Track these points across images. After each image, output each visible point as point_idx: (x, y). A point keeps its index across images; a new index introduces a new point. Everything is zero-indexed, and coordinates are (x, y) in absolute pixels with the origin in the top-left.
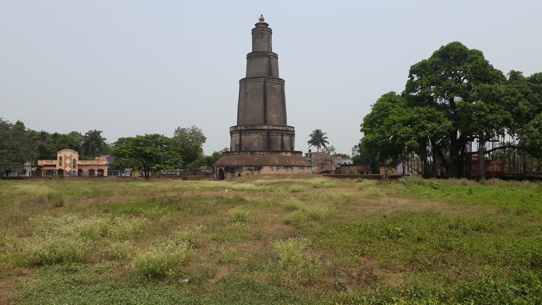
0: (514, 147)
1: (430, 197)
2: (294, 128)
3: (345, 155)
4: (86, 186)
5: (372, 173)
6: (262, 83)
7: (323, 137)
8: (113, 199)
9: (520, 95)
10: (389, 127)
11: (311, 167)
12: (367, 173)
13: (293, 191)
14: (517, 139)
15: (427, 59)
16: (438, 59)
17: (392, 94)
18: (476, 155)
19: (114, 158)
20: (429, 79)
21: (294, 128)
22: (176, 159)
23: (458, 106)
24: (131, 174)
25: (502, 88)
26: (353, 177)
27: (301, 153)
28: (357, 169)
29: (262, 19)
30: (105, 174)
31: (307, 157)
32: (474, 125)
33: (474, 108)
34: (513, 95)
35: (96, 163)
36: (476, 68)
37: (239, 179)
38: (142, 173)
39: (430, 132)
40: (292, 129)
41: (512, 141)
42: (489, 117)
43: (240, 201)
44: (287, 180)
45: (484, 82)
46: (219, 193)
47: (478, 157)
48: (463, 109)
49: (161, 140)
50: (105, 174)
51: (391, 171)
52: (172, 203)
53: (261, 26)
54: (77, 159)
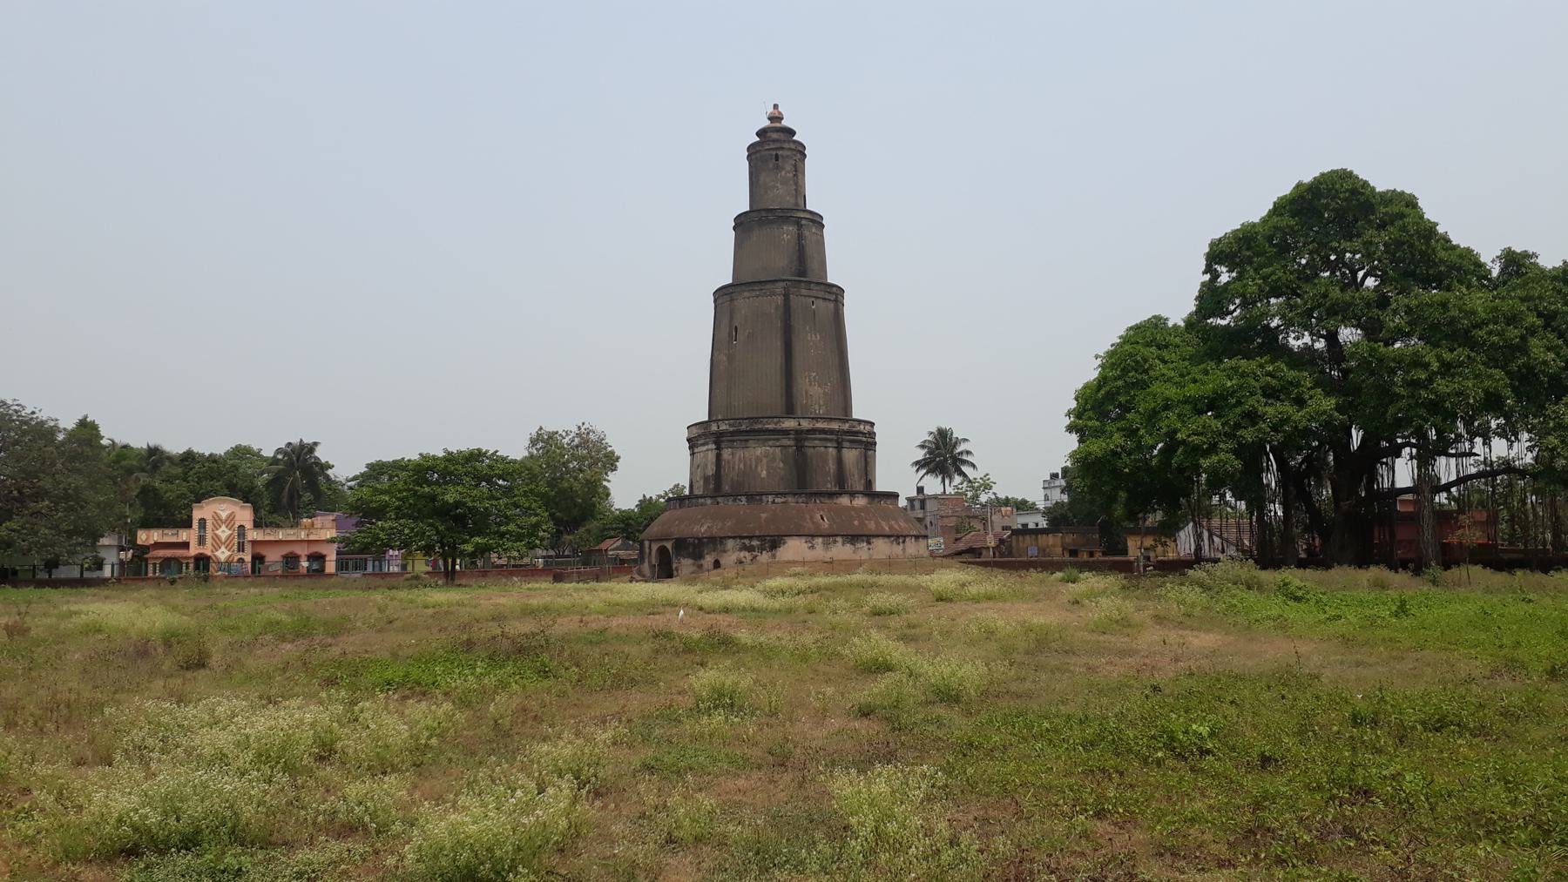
0: (1522, 473)
1: (1282, 625)
2: (872, 424)
3: (1024, 502)
4: (273, 603)
5: (1104, 554)
6: (780, 300)
7: (959, 449)
8: (350, 644)
9: (1532, 319)
10: (1152, 417)
11: (926, 537)
12: (1091, 554)
13: (877, 613)
14: (1530, 449)
15: (1256, 220)
16: (1287, 221)
17: (1157, 323)
18: (1409, 497)
19: (355, 520)
20: (1265, 278)
21: (872, 424)
22: (534, 519)
23: (1353, 355)
24: (404, 567)
25: (1479, 301)
26: (1050, 566)
27: (895, 496)
28: (1059, 542)
29: (776, 118)
30: (331, 567)
31: (913, 507)
32: (1400, 410)
33: (1399, 360)
34: (1512, 320)
35: (303, 536)
36: (1399, 243)
37: (715, 576)
38: (435, 561)
39: (1275, 428)
40: (868, 428)
41: (1513, 454)
42: (1442, 386)
43: (723, 644)
44: (857, 577)
45: (1426, 282)
46: (658, 622)
47: (1415, 502)
48: (1364, 364)
49: (490, 467)
50: (331, 567)
51: (1160, 549)
52: (524, 653)
53: (775, 136)
54: (249, 525)
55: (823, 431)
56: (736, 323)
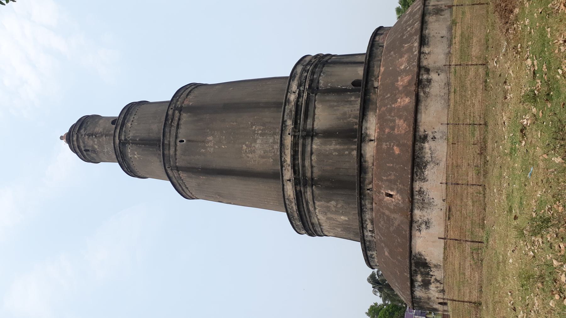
55: (294, 157)
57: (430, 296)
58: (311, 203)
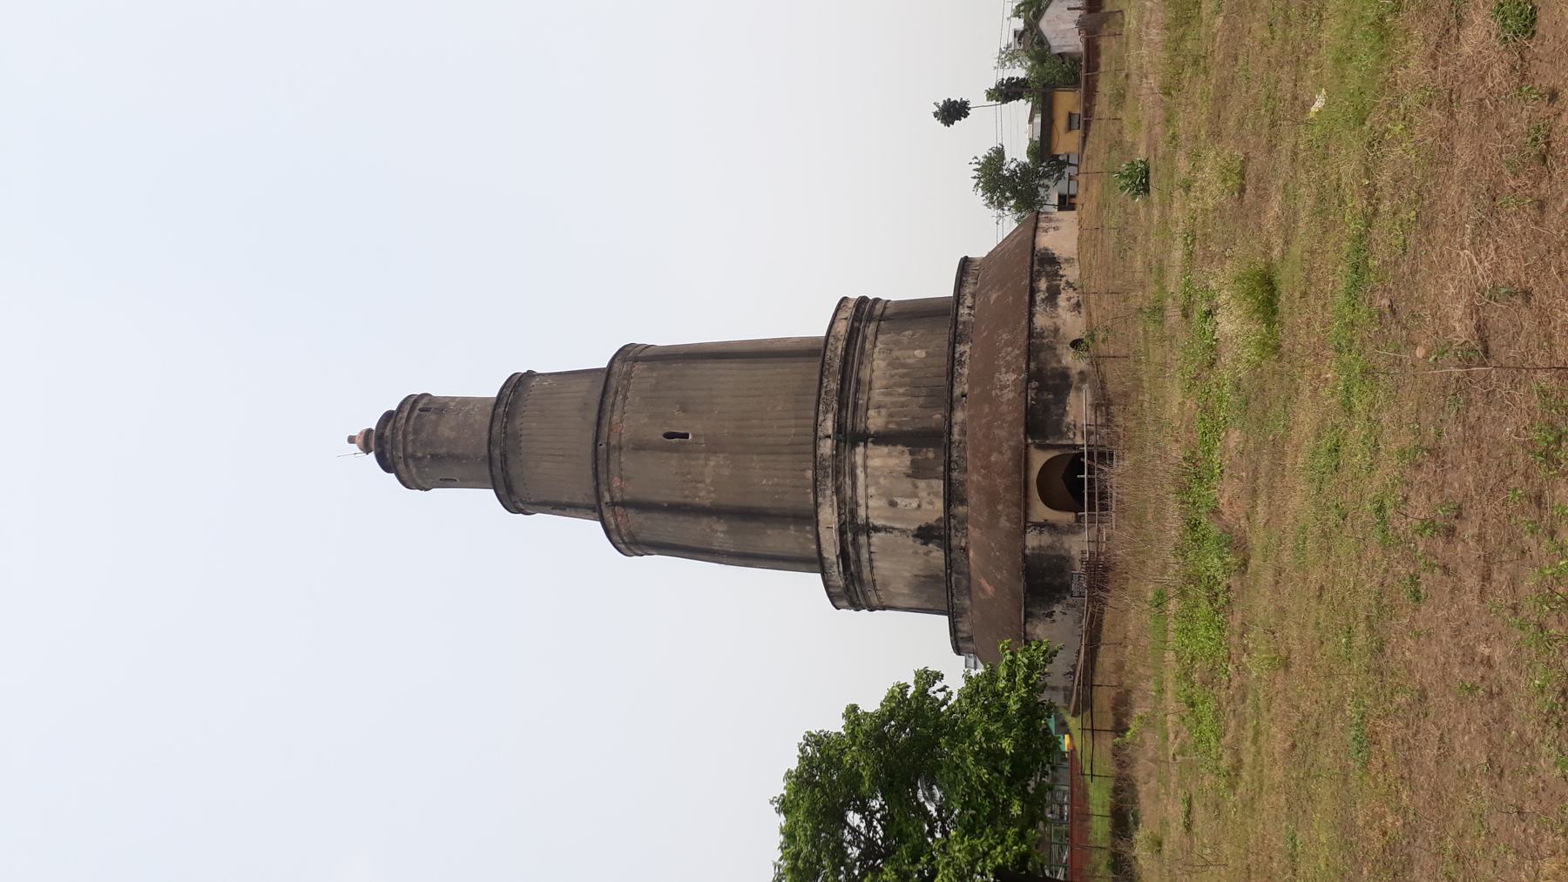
56: (657, 435)
57: (1059, 322)
58: (871, 338)
